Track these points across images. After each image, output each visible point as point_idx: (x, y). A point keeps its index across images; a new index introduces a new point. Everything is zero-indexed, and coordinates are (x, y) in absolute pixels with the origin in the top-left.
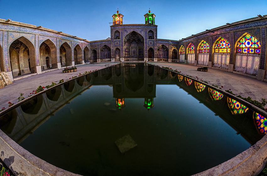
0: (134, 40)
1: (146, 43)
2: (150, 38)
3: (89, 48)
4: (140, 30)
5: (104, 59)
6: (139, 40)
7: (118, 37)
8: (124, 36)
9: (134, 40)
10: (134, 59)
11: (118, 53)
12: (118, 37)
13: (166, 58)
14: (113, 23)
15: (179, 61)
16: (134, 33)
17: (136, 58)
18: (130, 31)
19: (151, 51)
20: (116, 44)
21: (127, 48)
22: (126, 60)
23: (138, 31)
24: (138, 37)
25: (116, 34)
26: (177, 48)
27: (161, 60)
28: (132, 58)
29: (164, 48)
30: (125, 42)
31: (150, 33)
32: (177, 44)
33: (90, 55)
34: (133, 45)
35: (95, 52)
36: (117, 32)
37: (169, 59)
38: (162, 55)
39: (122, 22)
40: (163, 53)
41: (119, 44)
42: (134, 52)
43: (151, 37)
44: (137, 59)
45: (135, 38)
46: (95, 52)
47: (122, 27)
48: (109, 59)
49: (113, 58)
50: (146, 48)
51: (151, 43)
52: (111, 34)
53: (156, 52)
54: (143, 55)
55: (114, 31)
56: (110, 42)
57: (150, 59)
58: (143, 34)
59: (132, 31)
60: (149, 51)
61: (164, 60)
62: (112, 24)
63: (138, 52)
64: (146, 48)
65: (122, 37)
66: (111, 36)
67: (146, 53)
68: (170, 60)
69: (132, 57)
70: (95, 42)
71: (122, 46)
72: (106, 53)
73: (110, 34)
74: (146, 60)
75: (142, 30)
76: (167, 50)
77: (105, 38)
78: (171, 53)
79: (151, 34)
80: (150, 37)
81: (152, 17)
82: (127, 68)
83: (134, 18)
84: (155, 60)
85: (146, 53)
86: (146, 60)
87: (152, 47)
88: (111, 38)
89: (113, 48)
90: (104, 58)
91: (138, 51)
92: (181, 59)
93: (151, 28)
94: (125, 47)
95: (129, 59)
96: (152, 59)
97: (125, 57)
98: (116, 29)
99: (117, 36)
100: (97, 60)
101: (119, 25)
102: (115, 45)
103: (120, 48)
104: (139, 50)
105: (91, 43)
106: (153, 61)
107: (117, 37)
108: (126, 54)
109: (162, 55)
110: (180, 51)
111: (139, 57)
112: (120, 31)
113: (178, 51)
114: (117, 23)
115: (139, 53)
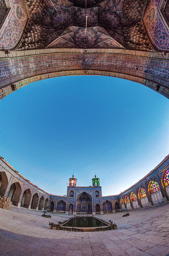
0: (84, 198)
1: (94, 200)
2: (97, 196)
3: (49, 199)
4: (89, 191)
5: (59, 211)
6: (88, 198)
7: (72, 196)
8: (77, 194)
9: (84, 198)
10: (84, 213)
11: (71, 208)
12: (72, 196)
13: (111, 210)
14: (70, 184)
15: (122, 210)
16: (84, 193)
17: (85, 212)
18: (81, 192)
19: (98, 206)
20: (70, 201)
21: (79, 204)
22: (78, 214)
23: (87, 192)
24: (87, 196)
25: (71, 193)
26: (118, 201)
27: (107, 212)
28: (83, 212)
29: (108, 203)
30: (77, 200)
31: (96, 193)
32: (118, 198)
33: (48, 204)
34: (83, 202)
35: (52, 203)
36: (72, 191)
37: (113, 211)
38: (107, 208)
39: (76, 184)
40: (108, 206)
41: (72, 201)
42: (84, 208)
43: (97, 196)
44: (86, 213)
45: (85, 197)
46: (52, 203)
47: (76, 188)
48: (63, 211)
49: (67, 211)
50: (94, 205)
51: (97, 200)
52: (67, 193)
53: (102, 207)
54: (91, 209)
55: (70, 191)
56: (66, 198)
57: (97, 212)
58: (91, 194)
59: (83, 191)
60: (96, 206)
61: (109, 212)
62: (68, 185)
63: (87, 208)
64: (94, 205)
65: (75, 196)
66: (67, 194)
67: (94, 208)
68: (114, 211)
69: (83, 211)
70: (54, 196)
71: (75, 202)
72: (62, 206)
73: (66, 193)
74: (94, 213)
75: (90, 191)
76: (111, 204)
77: (62, 195)
78: (114, 205)
79: (97, 193)
80: (96, 196)
81: (97, 180)
82: (78, 220)
83: (84, 182)
84: (101, 213)
85: (94, 208)
86: (94, 213)
87: (99, 203)
88: (67, 196)
89: (68, 204)
90: (59, 210)
91: (87, 206)
92: (123, 208)
93: (97, 188)
94: (77, 204)
95: (80, 213)
96: (99, 212)
97: (77, 211)
98: (72, 189)
99: (72, 195)
100: (54, 210)
101: (73, 187)
102: (69, 201)
103: (73, 204)
104: (88, 206)
105: (51, 196)
106: (100, 214)
107: (71, 195)
108: (77, 209)
109: (107, 208)
110: (121, 202)
111: (88, 211)
112: (74, 191)
113: (120, 202)
114: (72, 185)
115: (88, 208)
